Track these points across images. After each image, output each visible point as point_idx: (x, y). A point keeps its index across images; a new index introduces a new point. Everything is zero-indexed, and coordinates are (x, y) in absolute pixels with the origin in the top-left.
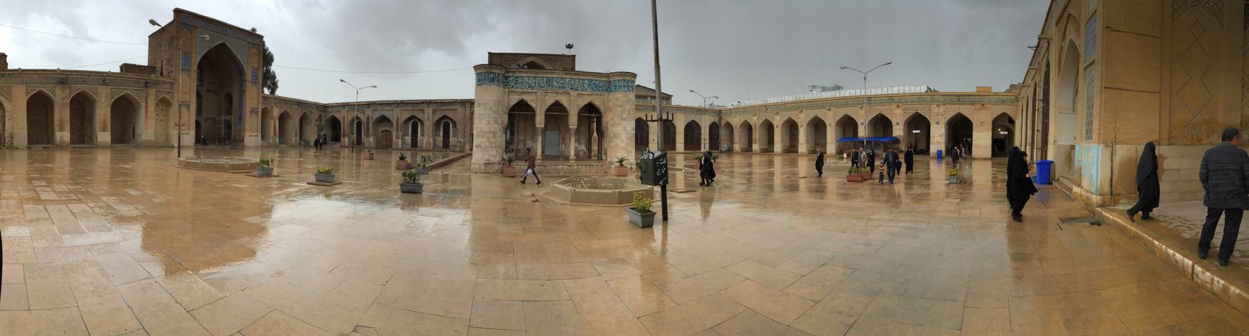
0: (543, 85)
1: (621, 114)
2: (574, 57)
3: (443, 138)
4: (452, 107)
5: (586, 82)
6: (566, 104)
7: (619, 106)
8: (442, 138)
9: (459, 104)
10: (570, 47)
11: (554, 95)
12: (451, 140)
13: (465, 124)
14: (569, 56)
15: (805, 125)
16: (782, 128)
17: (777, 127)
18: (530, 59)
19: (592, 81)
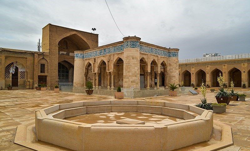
0: (150, 51)
1: (176, 67)
2: (97, 35)
3: (12, 78)
4: (22, 56)
5: (163, 52)
6: (157, 62)
7: (175, 64)
8: (11, 79)
9: (29, 55)
10: (94, 29)
11: (153, 56)
12: (19, 80)
13: (34, 69)
14: (95, 34)
15: (210, 73)
16: (195, 75)
17: (193, 74)
18: (74, 33)
19: (164, 51)
